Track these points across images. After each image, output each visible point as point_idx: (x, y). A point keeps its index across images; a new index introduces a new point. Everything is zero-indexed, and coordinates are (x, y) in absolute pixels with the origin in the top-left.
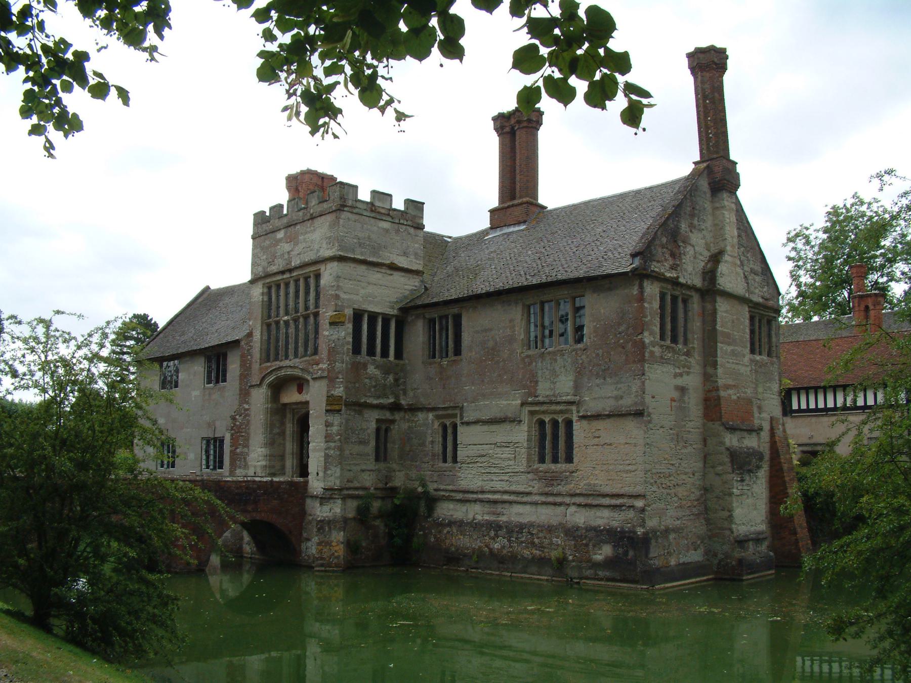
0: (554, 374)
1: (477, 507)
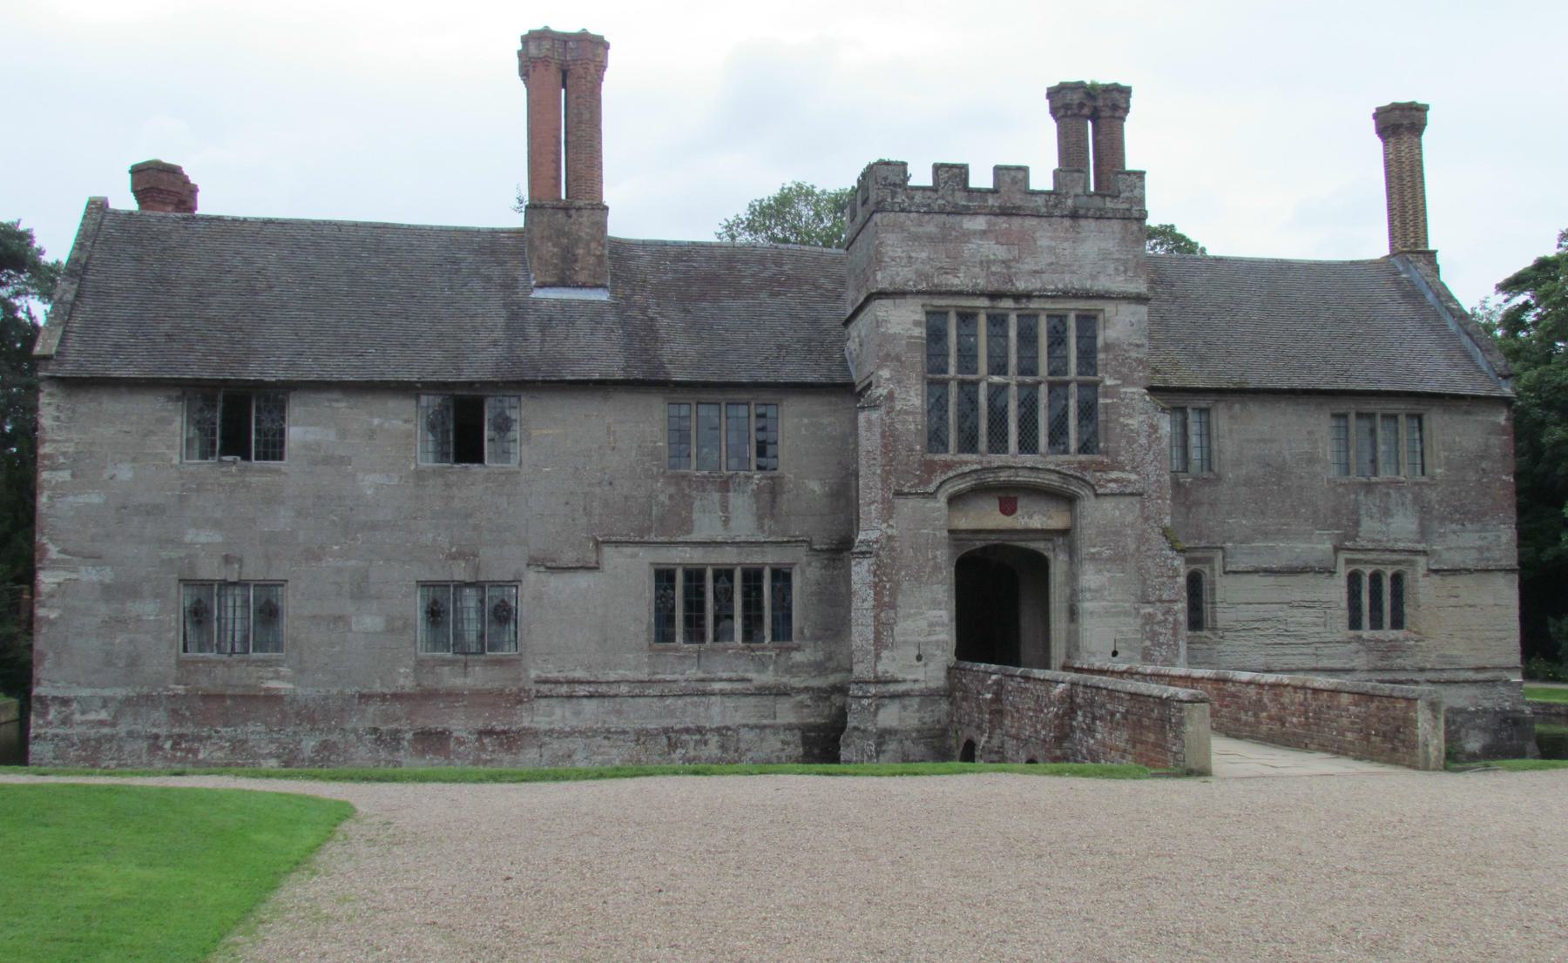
0: (1386, 513)
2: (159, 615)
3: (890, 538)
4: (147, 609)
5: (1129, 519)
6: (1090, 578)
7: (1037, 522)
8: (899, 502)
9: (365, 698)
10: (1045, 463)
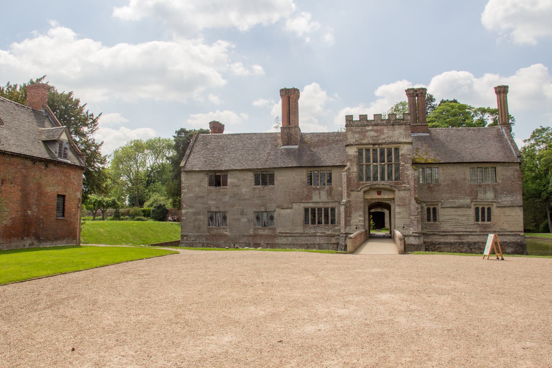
0: (485, 192)
1: (451, 237)
2: (203, 218)
3: (350, 201)
4: (202, 217)
5: (407, 196)
6: (398, 209)
7: (386, 197)
8: (352, 193)
9: (244, 236)
10: (385, 183)
